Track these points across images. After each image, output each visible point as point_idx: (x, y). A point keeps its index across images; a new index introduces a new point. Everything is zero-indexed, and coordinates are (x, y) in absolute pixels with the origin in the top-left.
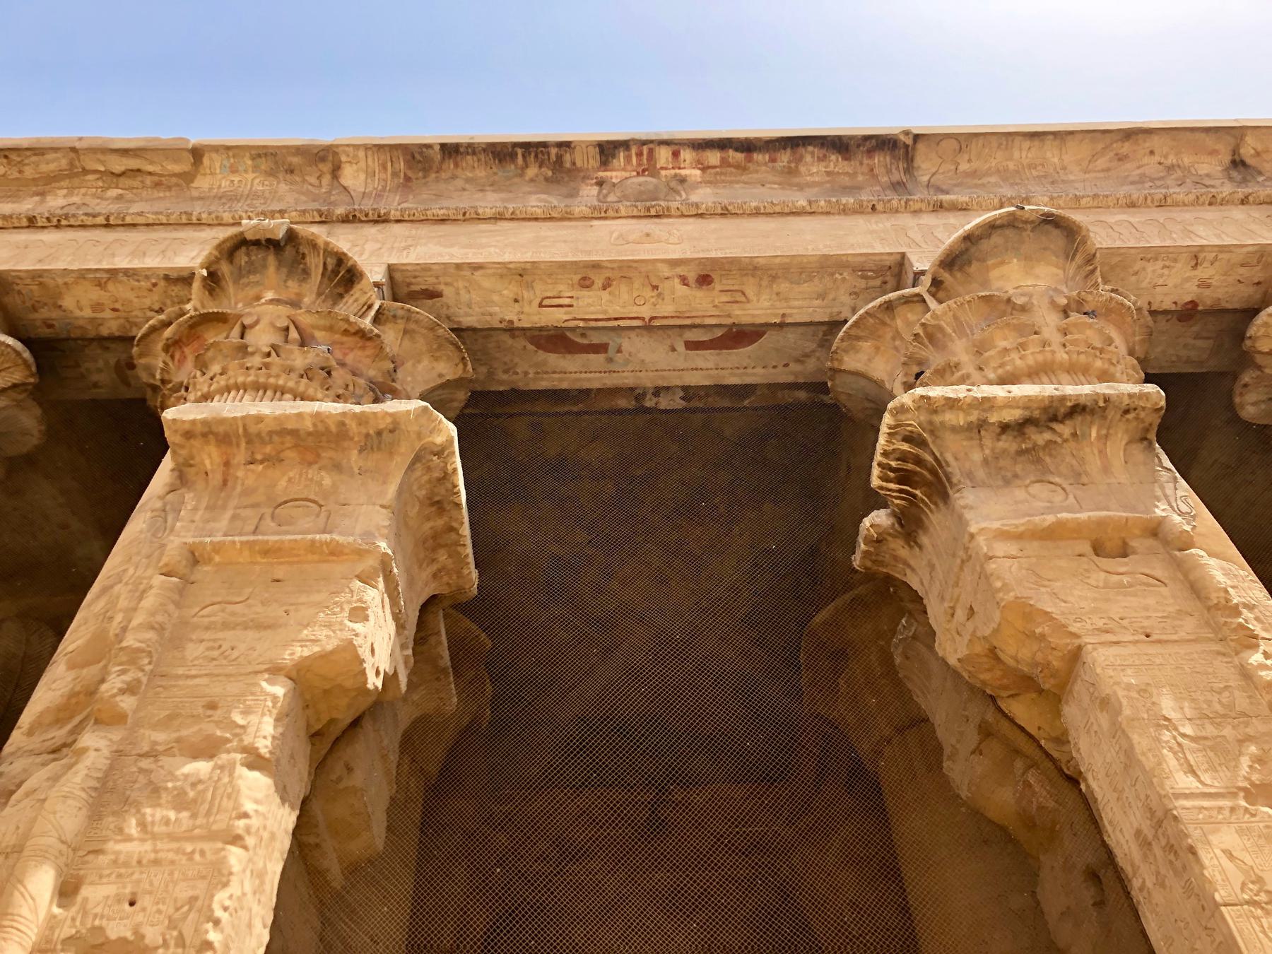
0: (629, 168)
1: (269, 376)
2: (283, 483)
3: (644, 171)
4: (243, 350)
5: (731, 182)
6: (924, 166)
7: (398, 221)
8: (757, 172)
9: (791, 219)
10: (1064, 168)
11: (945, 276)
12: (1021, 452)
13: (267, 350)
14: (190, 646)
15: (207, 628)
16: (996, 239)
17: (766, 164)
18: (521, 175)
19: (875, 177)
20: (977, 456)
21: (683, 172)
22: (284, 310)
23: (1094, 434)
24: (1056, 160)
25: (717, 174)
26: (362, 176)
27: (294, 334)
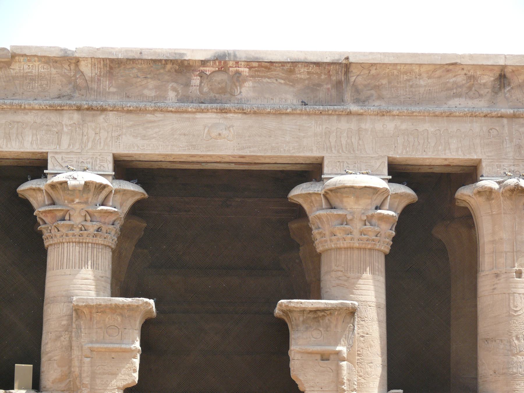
0: (215, 66)
1: (83, 239)
2: (107, 320)
3: (221, 68)
4: (72, 227)
5: (262, 77)
6: (354, 71)
7: (111, 111)
8: (275, 70)
9: (283, 117)
10: (420, 75)
11: (329, 192)
12: (314, 318)
13: (80, 226)
14: (97, 380)
15: (99, 374)
16: (346, 190)
17: (279, 67)
18: (164, 68)
19: (330, 76)
20: (301, 319)
21: (240, 69)
22: (82, 206)
23: (336, 313)
24: (417, 70)
25: (256, 71)
26: (90, 66)
27: (88, 218)
